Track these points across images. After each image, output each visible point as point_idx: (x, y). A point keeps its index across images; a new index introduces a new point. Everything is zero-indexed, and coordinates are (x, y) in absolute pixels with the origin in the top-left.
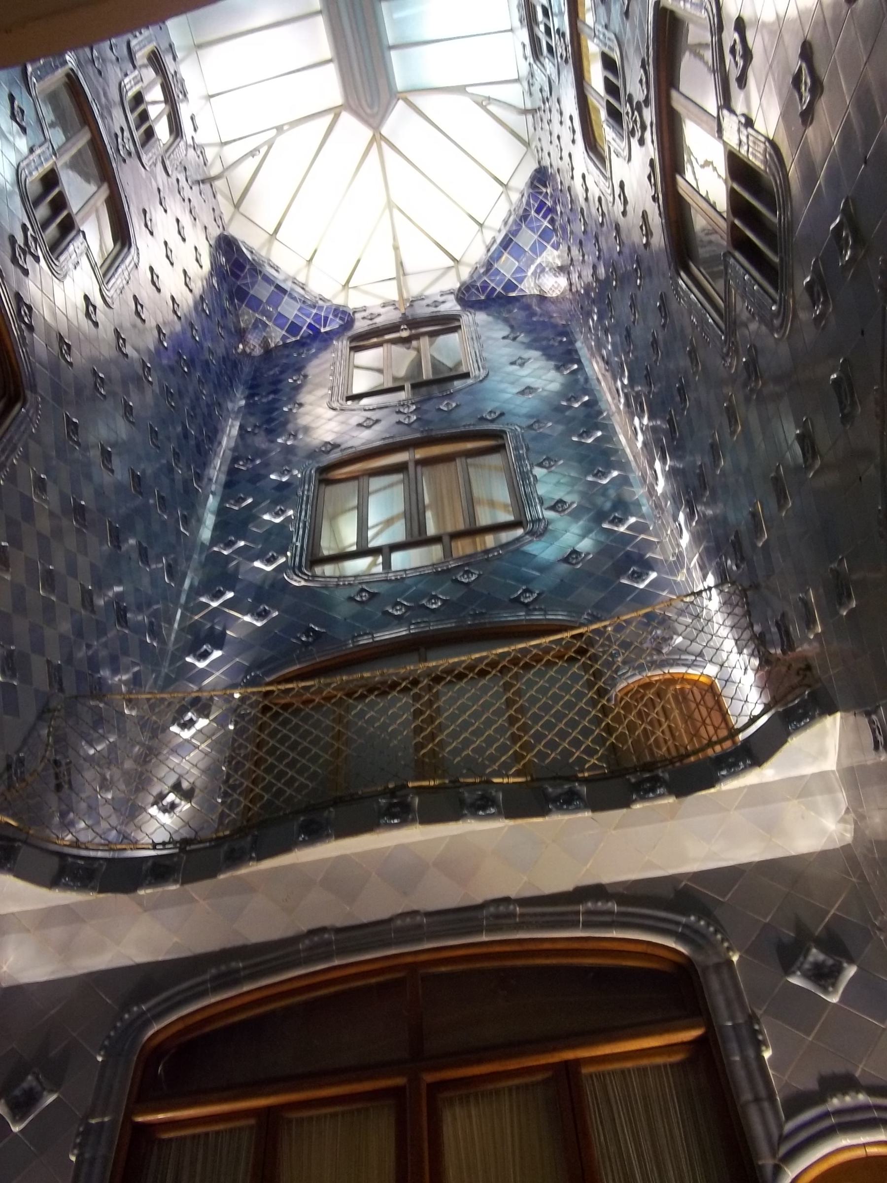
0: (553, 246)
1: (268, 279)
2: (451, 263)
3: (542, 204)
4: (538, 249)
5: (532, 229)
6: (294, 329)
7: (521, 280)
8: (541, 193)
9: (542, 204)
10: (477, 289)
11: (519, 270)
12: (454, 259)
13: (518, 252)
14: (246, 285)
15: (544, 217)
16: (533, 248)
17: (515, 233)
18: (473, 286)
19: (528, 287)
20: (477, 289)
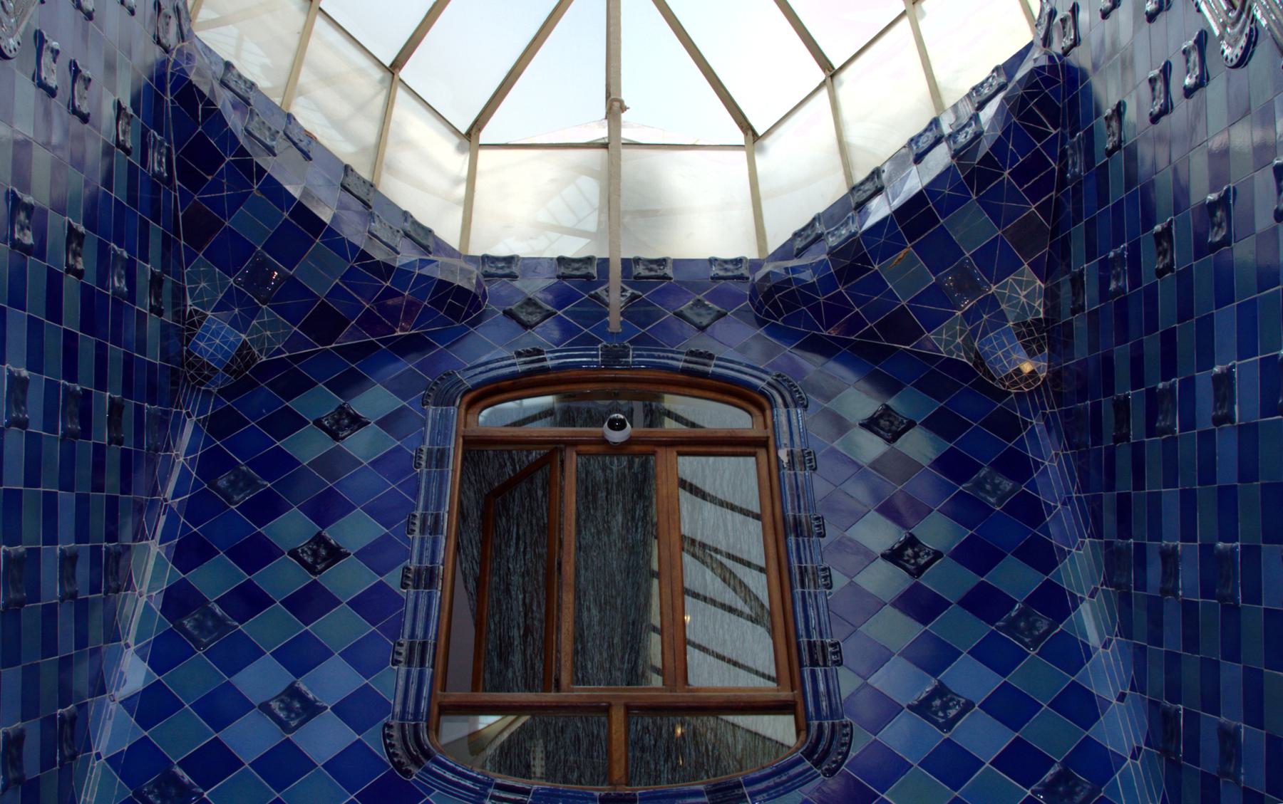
0: (1035, 267)
1: (275, 191)
2: (738, 137)
3: (1037, 163)
4: (996, 261)
5: (995, 215)
6: (324, 323)
7: (933, 322)
8: (1041, 135)
9: (1037, 163)
10: (816, 310)
11: (936, 293)
12: (745, 126)
13: (940, 252)
14: (216, 204)
15: (1034, 194)
16: (983, 256)
17: (950, 205)
18: (807, 300)
19: (946, 340)
20: (816, 310)
